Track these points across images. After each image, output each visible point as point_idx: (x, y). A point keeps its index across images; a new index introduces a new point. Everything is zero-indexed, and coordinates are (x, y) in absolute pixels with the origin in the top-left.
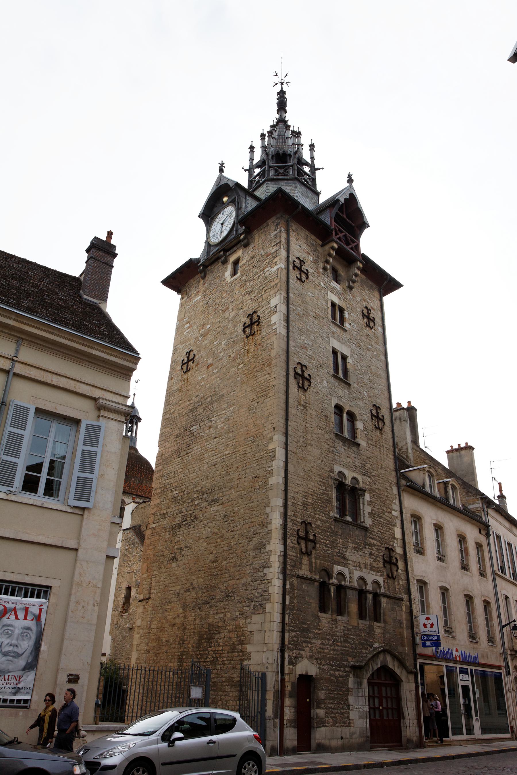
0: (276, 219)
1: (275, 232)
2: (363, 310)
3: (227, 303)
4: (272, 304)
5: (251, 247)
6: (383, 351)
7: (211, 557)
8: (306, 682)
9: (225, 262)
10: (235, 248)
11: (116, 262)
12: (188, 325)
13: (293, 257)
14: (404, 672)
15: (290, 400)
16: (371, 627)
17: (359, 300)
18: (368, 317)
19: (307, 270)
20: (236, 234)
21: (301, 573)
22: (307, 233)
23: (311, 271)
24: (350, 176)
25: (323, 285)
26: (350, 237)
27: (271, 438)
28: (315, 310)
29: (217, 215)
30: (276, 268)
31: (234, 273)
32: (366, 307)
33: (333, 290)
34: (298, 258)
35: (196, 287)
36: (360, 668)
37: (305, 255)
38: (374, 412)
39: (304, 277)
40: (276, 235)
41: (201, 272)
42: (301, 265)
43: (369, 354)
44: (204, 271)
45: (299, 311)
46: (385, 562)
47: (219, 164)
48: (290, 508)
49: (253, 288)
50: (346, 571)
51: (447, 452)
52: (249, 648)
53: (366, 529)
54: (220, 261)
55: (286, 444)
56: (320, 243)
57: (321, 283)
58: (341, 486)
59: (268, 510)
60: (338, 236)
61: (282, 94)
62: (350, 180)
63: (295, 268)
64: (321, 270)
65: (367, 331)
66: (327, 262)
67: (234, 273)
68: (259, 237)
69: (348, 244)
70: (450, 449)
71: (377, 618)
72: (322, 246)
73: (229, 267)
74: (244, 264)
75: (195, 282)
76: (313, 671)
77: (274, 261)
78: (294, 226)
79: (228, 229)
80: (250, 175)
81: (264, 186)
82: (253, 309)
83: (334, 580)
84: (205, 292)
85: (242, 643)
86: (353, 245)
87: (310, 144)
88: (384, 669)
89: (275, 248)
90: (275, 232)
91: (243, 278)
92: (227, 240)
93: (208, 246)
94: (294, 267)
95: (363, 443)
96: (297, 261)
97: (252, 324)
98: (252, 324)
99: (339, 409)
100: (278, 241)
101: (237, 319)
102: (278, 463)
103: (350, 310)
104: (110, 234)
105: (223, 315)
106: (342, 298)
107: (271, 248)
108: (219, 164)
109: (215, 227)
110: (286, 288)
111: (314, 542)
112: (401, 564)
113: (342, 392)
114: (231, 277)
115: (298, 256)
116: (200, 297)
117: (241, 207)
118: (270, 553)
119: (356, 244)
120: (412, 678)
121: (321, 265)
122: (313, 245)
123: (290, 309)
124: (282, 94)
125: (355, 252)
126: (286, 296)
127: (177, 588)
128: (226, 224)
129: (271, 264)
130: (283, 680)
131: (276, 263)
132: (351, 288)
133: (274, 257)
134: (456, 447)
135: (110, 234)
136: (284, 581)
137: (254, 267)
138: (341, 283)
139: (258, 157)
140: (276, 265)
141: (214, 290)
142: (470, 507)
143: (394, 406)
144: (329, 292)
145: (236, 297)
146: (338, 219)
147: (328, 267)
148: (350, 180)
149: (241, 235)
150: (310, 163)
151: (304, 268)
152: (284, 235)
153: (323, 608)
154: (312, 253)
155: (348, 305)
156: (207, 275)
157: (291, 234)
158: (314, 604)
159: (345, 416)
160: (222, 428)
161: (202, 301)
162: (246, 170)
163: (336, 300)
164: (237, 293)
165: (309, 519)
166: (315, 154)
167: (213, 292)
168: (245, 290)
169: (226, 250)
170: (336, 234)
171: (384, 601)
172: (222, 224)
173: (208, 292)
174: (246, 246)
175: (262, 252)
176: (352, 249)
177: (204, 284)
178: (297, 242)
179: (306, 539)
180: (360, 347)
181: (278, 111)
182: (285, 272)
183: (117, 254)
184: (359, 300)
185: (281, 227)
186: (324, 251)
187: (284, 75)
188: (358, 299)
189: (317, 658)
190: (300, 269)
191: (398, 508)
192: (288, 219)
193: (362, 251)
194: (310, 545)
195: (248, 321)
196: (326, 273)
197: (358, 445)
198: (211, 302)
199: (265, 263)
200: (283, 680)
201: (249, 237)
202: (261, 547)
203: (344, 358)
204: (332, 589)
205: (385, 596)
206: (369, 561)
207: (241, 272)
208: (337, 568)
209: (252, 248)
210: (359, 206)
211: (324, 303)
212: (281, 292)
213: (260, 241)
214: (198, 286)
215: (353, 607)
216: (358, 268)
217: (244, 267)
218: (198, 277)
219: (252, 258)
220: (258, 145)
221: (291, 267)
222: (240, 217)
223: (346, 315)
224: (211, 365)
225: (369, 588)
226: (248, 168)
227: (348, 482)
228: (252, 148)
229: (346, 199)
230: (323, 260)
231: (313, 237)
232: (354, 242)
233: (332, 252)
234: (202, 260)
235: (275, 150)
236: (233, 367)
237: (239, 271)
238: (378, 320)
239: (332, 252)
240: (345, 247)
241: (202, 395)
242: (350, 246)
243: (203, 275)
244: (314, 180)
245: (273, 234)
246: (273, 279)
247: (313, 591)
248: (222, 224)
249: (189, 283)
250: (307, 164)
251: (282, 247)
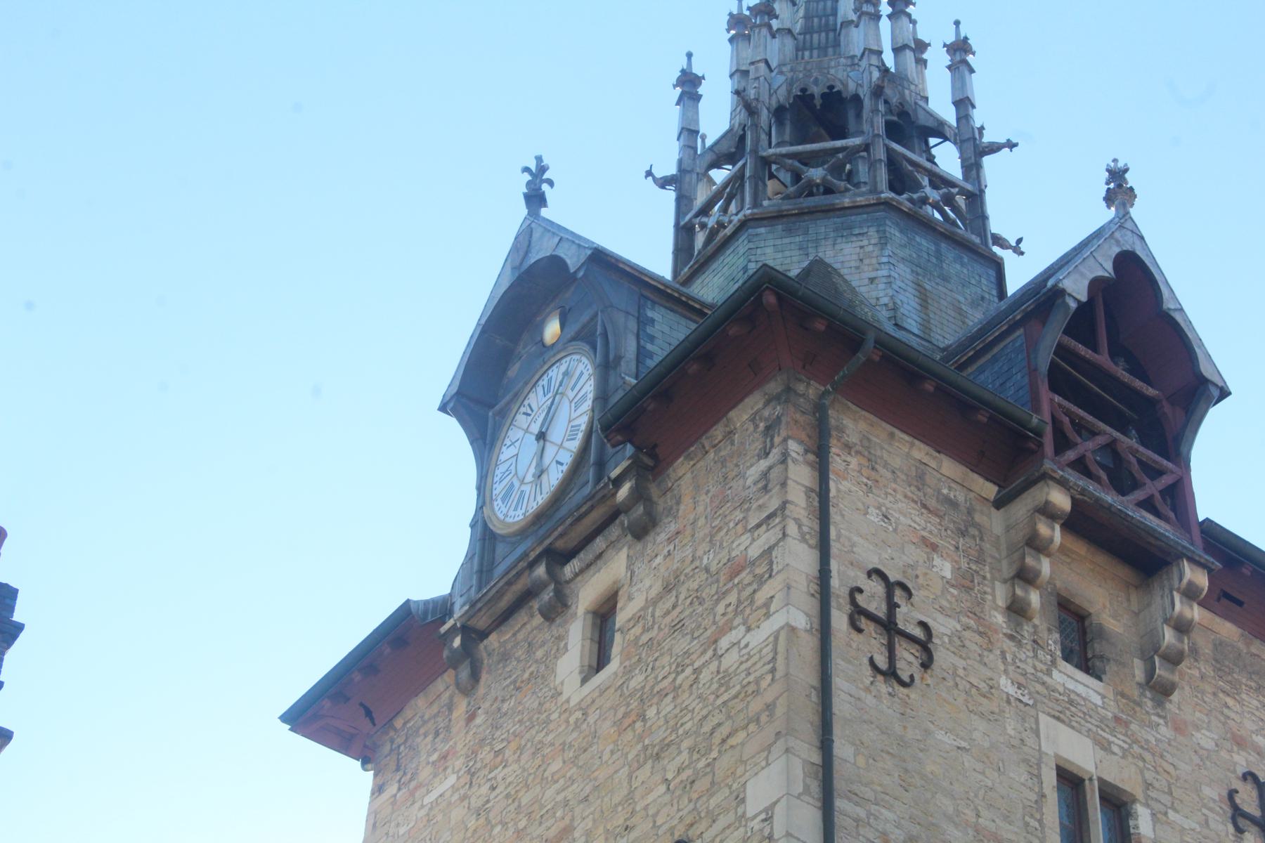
0: (766, 404)
1: (763, 464)
2: (1232, 794)
3: (566, 803)
4: (753, 806)
5: (662, 537)
9: (557, 609)
10: (599, 543)
13: (851, 573)
17: (1210, 745)
19: (923, 625)
20: (599, 478)
22: (921, 451)
23: (943, 626)
24: (1117, 175)
25: (1011, 690)
26: (1134, 452)
28: (970, 815)
29: (518, 397)
30: (768, 627)
32: (1249, 776)
33: (1068, 710)
34: (876, 573)
35: (437, 734)
37: (915, 554)
39: (907, 659)
40: (765, 475)
42: (892, 606)
44: (468, 651)
45: (889, 827)
47: (526, 170)
49: (675, 729)
54: (536, 604)
56: (991, 490)
57: (1004, 683)
60: (1071, 455)
62: (1119, 190)
63: (863, 623)
64: (999, 619)
67: (601, 660)
68: (697, 488)
69: (1122, 481)
72: (999, 503)
73: (577, 633)
74: (637, 618)
75: (435, 709)
77: (761, 597)
78: (853, 425)
79: (567, 459)
80: (683, 201)
81: (742, 245)
82: (672, 829)
84: (475, 753)
86: (1152, 488)
87: (950, 39)
89: (767, 537)
90: (763, 464)
91: (633, 684)
92: (564, 511)
93: (483, 539)
94: (858, 614)
96: (874, 588)
100: (774, 504)
103: (1166, 799)
106: (1118, 742)
107: (745, 539)
108: (526, 170)
109: (512, 451)
110: (816, 719)
114: (584, 681)
115: (874, 562)
116: (452, 779)
117: (619, 358)
119: (1165, 481)
121: (1001, 595)
122: (953, 504)
123: (839, 820)
125: (1167, 520)
126: (816, 758)
128: (556, 434)
129: (749, 611)
131: (767, 605)
132: (1163, 691)
133: (761, 581)
137: (677, 627)
138: (1111, 668)
139: (717, 117)
140: (768, 615)
141: (513, 745)
144: (1043, 719)
145: (602, 775)
147: (1035, 598)
148: (1119, 190)
149: (618, 482)
150: (953, 122)
151: (907, 618)
152: (801, 475)
154: (946, 544)
155: (1149, 776)
156: (484, 677)
157: (837, 460)
161: (463, 798)
162: (664, 183)
163: (1082, 755)
164: (606, 757)
166: (979, 87)
167: (508, 753)
168: (641, 738)
169: (557, 557)
170: (1062, 444)
172: (541, 436)
173: (485, 755)
174: (640, 532)
175: (711, 560)
177: (471, 717)
178: (871, 499)
182: (808, 645)
183: (20, 627)
184: (1210, 745)
185: (785, 440)
186: (1008, 529)
188: (1205, 739)
190: (889, 626)
192: (823, 395)
193: (1204, 510)
196: (1027, 629)
199: (720, 608)
201: (654, 490)
207: (626, 656)
209: (670, 540)
210: (1168, 305)
211: (1020, 775)
212: (792, 742)
213: (700, 508)
214: (448, 728)
216: (1190, 593)
217: (637, 630)
218: (444, 684)
219: (667, 589)
221: (840, 620)
222: (614, 399)
226: (672, 170)
228: (689, 85)
229: (1097, 285)
230: (1007, 570)
231: (950, 467)
233: (1043, 529)
234: (458, 602)
235: (790, 83)
237: (616, 650)
239: (1043, 529)
240: (1110, 498)
242: (1139, 495)
243: (464, 673)
244: (976, 198)
245: (754, 472)
246: (757, 681)
248: (541, 436)
249: (408, 713)
250: (939, 130)
251: (792, 529)
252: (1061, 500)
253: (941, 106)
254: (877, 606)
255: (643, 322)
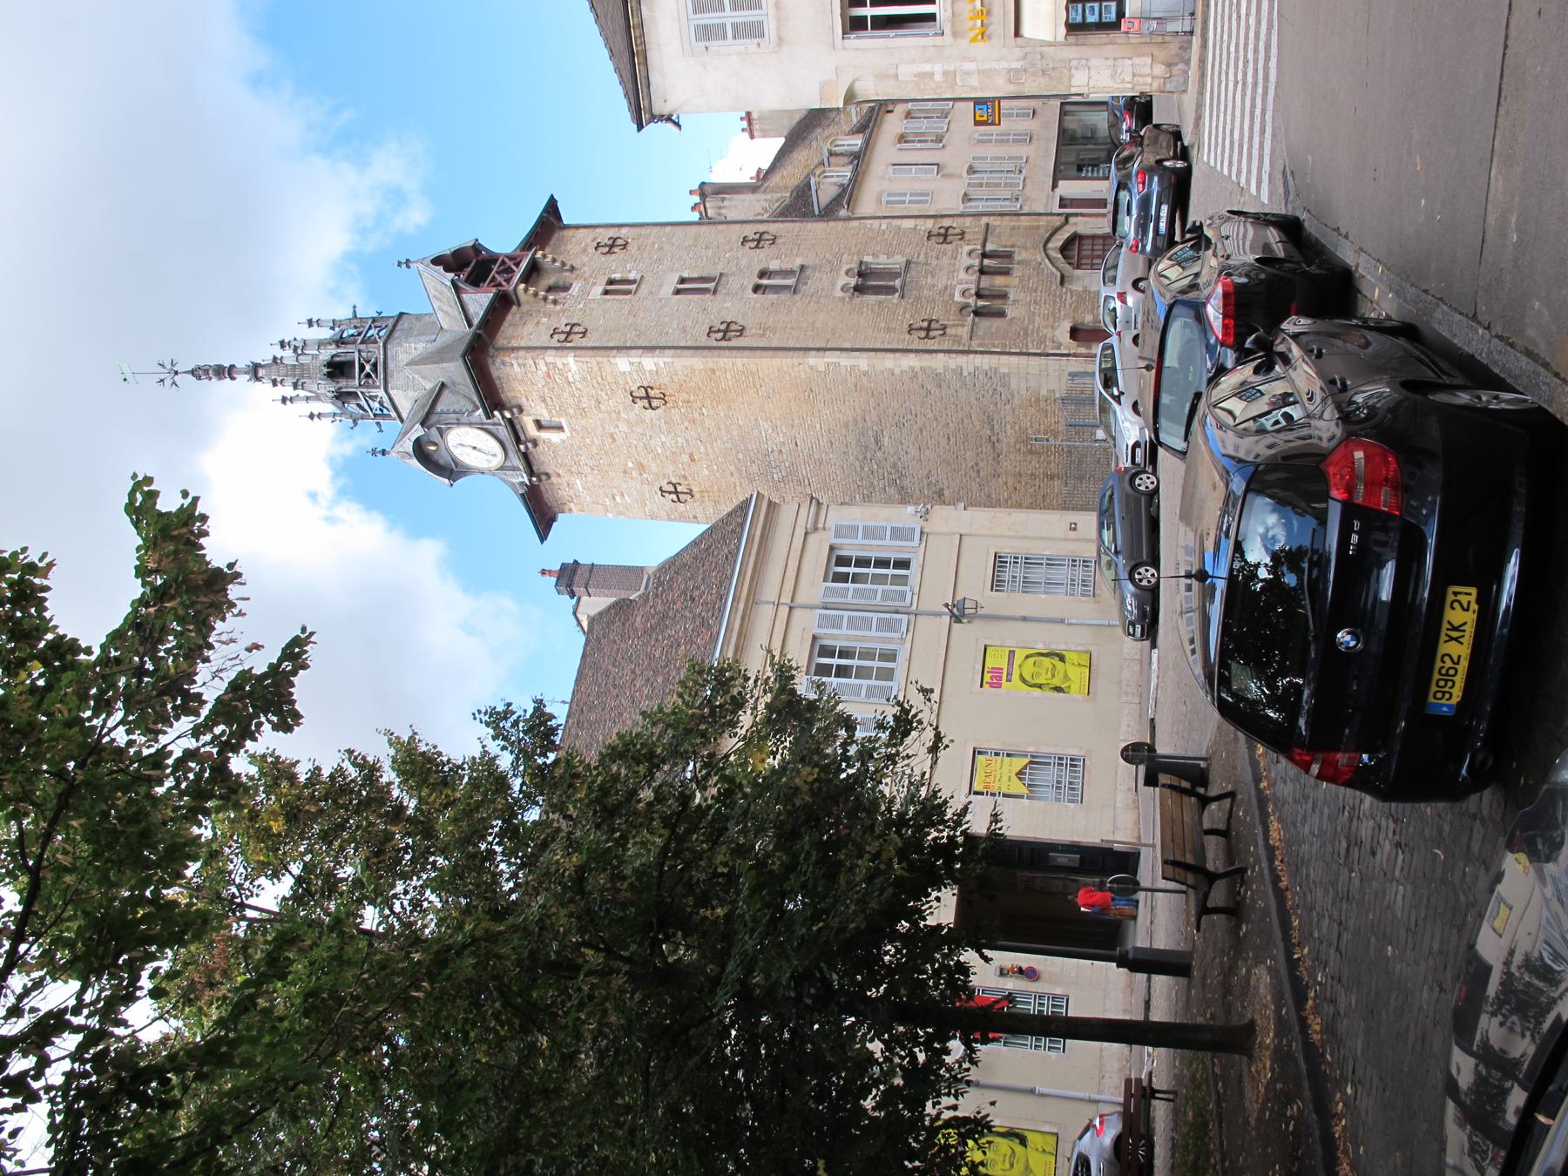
6: (656, 229)
7: (943, 442)
8: (1075, 333)
11: (584, 560)
12: (618, 499)
14: (1067, 228)
15: (761, 345)
16: (1020, 263)
18: (612, 246)
21: (966, 336)
22: (506, 324)
27: (811, 368)
31: (560, 428)
33: (585, 292)
36: (1062, 277)
38: (753, 244)
39: (576, 329)
41: (540, 480)
43: (667, 247)
46: (944, 241)
48: (894, 346)
50: (960, 288)
51: (752, 137)
52: (1044, 392)
53: (908, 263)
55: (818, 350)
56: (514, 308)
58: (858, 289)
59: (897, 372)
61: (196, 373)
65: (632, 248)
66: (545, 299)
69: (509, 271)
70: (746, 135)
71: (1008, 256)
73: (544, 435)
76: (1066, 326)
78: (501, 341)
83: (972, 301)
85: (1038, 401)
86: (510, 263)
88: (1064, 249)
94: (566, 340)
95: (799, 261)
96: (556, 337)
97: (648, 397)
98: (648, 397)
99: (756, 289)
101: (633, 418)
102: (845, 361)
104: (543, 572)
105: (620, 441)
111: (930, 321)
112: (946, 223)
113: (733, 283)
118: (946, 369)
120: (1072, 220)
124: (196, 373)
127: (975, 487)
130: (1075, 355)
132: (572, 269)
134: (745, 124)
135: (543, 572)
136: (976, 352)
137: (559, 397)
139: (329, 408)
142: (855, 120)
143: (695, 217)
146: (476, 280)
152: (522, 353)
153: (1001, 314)
157: (514, 343)
158: (996, 323)
159: (765, 282)
160: (785, 435)
163: (599, 289)
165: (906, 327)
171: (990, 247)
174: (521, 410)
176: (517, 265)
179: (928, 329)
180: (660, 260)
181: (233, 378)
187: (160, 369)
188: (585, 259)
189: (1055, 318)
190: (569, 334)
191: (877, 222)
194: (934, 325)
195: (641, 403)
197: (802, 267)
198: (591, 463)
200: (1075, 355)
202: (938, 380)
203: (683, 281)
204: (981, 303)
205: (984, 245)
206: (945, 260)
208: (958, 298)
215: (999, 281)
216: (544, 256)
219: (544, 401)
220: (305, 408)
223: (617, 276)
224: (691, 456)
225: (977, 262)
227: (853, 281)
229: (447, 270)
231: (509, 317)
232: (503, 262)
236: (703, 422)
238: (612, 233)
241: (732, 468)
247: (985, 323)
252: (522, 286)
253: (326, 333)
254: (563, 337)
255: (442, 412)
